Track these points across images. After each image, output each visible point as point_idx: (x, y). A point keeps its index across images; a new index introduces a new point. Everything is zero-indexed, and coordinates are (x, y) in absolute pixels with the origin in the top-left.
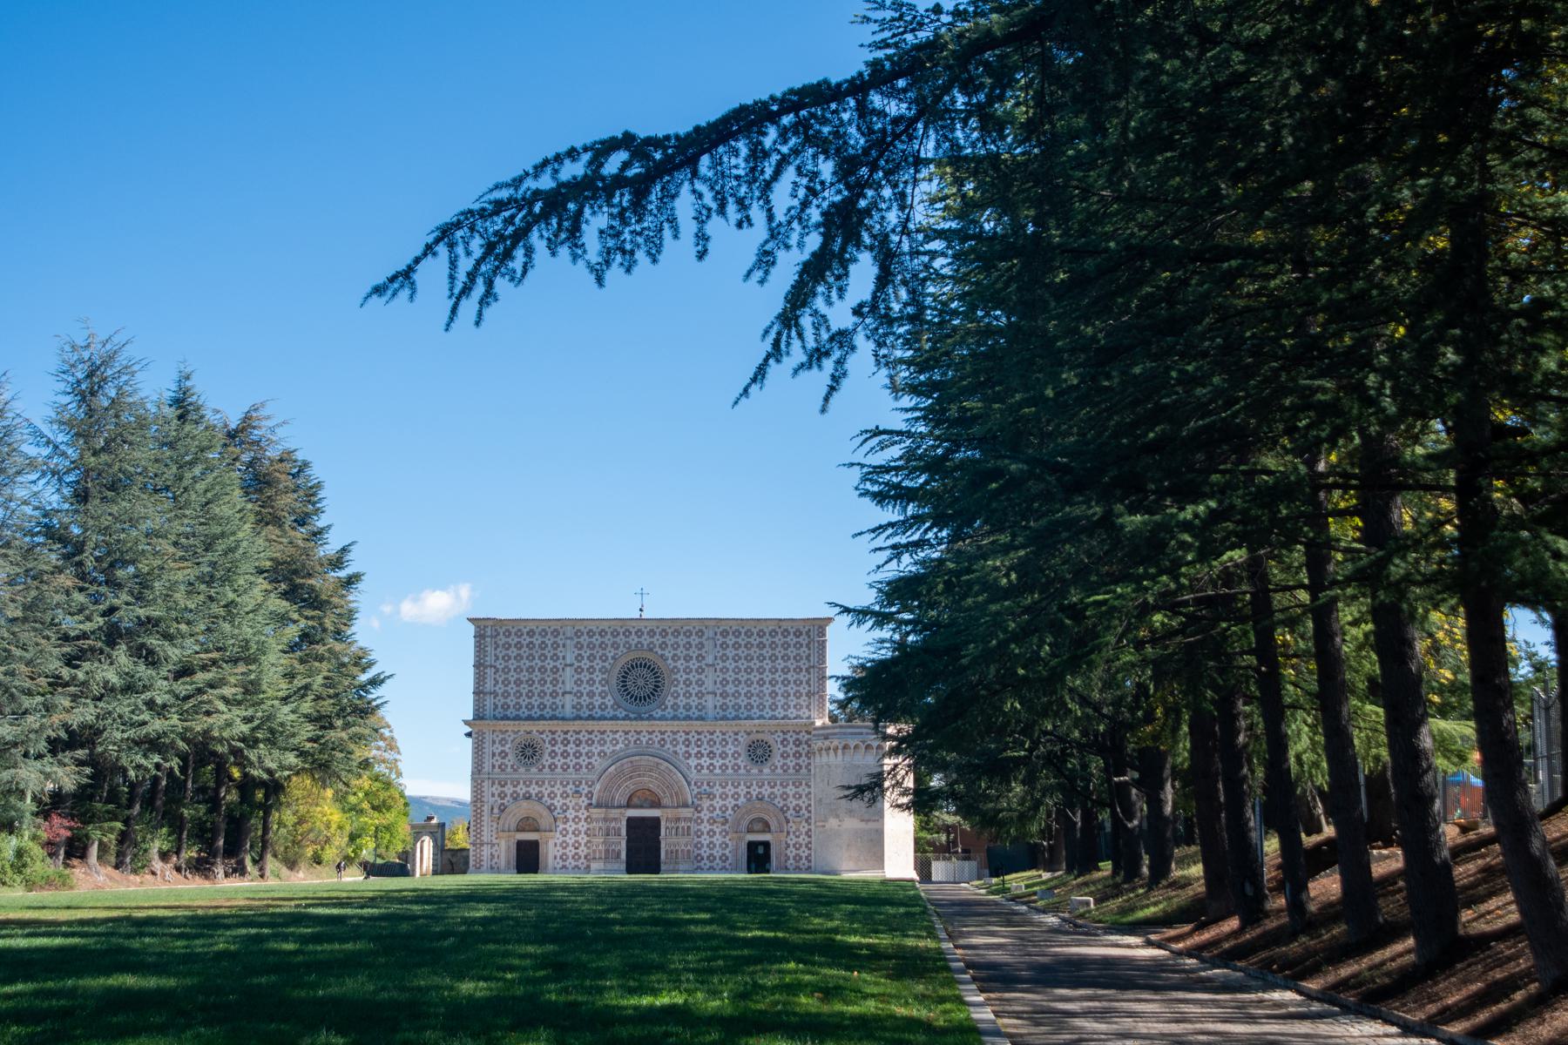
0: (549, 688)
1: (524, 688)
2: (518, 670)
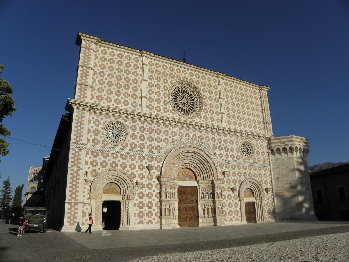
0: (131, 92)
1: (114, 89)
2: (110, 76)
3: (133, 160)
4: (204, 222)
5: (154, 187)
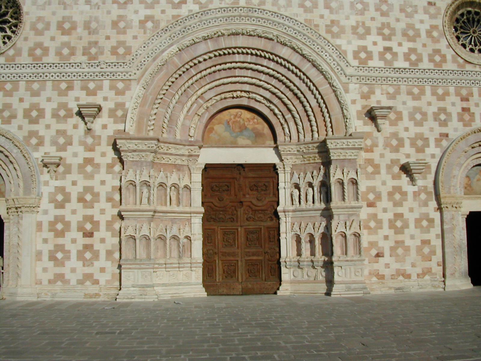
3: (35, 94)
4: (299, 282)
5: (103, 170)
